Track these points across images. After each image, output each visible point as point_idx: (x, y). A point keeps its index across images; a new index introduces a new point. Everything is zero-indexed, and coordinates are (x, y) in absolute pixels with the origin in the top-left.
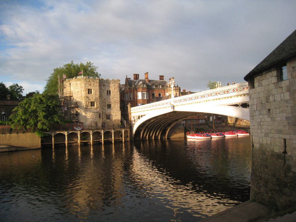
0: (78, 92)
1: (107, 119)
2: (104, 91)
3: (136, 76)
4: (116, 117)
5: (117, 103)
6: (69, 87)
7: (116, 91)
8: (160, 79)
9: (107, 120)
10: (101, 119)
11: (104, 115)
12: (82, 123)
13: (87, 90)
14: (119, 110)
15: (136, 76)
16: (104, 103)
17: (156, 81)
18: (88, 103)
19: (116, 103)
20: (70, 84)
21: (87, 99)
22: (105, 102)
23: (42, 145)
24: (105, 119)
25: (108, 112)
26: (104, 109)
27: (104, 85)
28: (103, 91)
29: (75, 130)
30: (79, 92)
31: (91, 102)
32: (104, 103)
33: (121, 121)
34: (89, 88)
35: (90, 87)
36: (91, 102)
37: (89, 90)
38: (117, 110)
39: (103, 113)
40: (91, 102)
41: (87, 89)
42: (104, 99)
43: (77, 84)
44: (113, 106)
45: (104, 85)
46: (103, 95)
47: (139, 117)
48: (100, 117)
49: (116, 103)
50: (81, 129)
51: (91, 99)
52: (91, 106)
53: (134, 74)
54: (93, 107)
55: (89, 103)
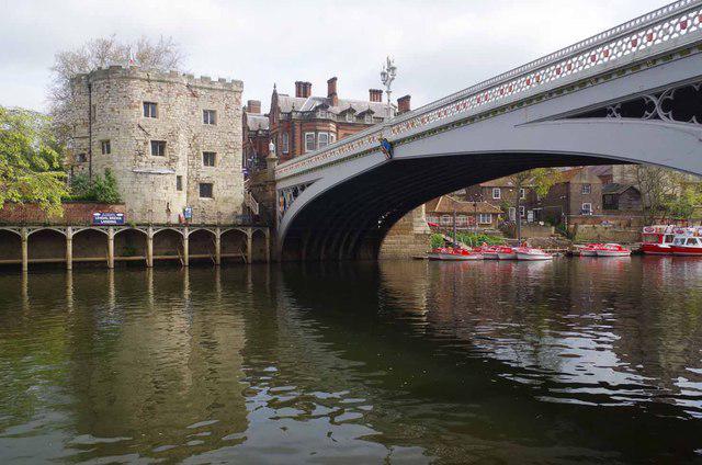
0: (113, 110)
1: (202, 195)
2: (193, 113)
3: (303, 89)
6: (88, 97)
8: (372, 99)
12: (124, 204)
15: (303, 89)
16: (194, 149)
17: (359, 104)
18: (141, 143)
20: (90, 86)
21: (141, 132)
22: (197, 146)
27: (194, 95)
31: (152, 142)
32: (194, 149)
33: (245, 207)
34: (146, 100)
35: (149, 98)
39: (189, 178)
40: (152, 142)
41: (139, 102)
47: (296, 194)
48: (179, 187)
51: (152, 133)
52: (154, 153)
53: (298, 84)
55: (146, 143)
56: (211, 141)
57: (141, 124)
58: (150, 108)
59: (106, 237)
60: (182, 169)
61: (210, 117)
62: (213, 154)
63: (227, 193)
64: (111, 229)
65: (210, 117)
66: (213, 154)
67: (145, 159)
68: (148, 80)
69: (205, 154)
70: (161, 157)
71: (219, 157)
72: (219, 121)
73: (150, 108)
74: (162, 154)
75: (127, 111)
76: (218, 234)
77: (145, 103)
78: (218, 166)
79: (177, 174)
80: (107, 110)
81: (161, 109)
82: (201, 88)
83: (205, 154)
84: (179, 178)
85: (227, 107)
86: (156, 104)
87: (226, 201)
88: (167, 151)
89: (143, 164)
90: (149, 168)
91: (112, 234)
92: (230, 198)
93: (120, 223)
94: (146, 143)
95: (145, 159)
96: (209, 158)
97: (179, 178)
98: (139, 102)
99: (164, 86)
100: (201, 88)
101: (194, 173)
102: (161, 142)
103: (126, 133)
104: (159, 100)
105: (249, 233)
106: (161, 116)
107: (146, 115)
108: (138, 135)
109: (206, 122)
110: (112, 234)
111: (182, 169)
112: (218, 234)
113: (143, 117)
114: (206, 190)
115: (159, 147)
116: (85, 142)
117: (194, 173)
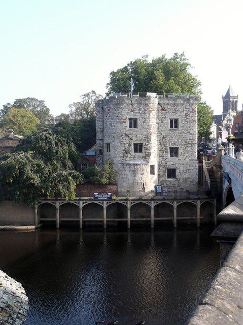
0: (111, 125)
4: (187, 174)
5: (190, 145)
7: (188, 120)
9: (169, 179)
10: (155, 177)
11: (163, 170)
13: (128, 121)
14: (197, 158)
18: (127, 145)
19: (188, 145)
20: (103, 108)
21: (127, 138)
22: (165, 144)
23: (41, 222)
24: (165, 178)
25: (172, 163)
26: (163, 157)
28: (160, 122)
29: (96, 199)
30: (113, 125)
35: (132, 116)
36: (136, 145)
37: (130, 119)
38: (190, 158)
39: (159, 165)
41: (126, 119)
42: (163, 138)
43: (109, 110)
44: (182, 151)
45: (163, 109)
46: (161, 128)
48: (152, 172)
49: (188, 145)
50: (108, 197)
51: (134, 138)
52: (136, 151)
54: (138, 154)
56: (176, 139)
57: (127, 133)
58: (133, 123)
59: (102, 208)
60: (154, 160)
61: (174, 124)
62: (177, 149)
63: (187, 175)
64: (105, 202)
65: (174, 124)
66: (177, 149)
67: (129, 155)
68: (132, 104)
69: (171, 149)
70: (141, 153)
71: (181, 151)
72: (180, 125)
73: (133, 123)
74: (141, 151)
75: (119, 125)
76: (175, 205)
77: (130, 119)
78: (180, 157)
79: (150, 164)
80: (108, 124)
81: (139, 122)
82: (168, 104)
83: (171, 149)
84: (152, 167)
85: (186, 116)
86: (137, 119)
87: (185, 180)
88: (143, 149)
89: (128, 159)
90: (132, 162)
91: (105, 205)
92: (189, 178)
93: (110, 199)
94: (130, 145)
95: (129, 155)
96: (174, 152)
97: (152, 167)
98: (126, 119)
99: (141, 107)
100: (168, 104)
101: (163, 162)
102: (140, 143)
103: (118, 139)
104: (138, 116)
105: (199, 204)
106: (139, 127)
107: (131, 126)
108: (126, 140)
109: (171, 126)
110: (105, 205)
111: (154, 160)
112: (175, 205)
113: (128, 128)
114: (172, 173)
115: (139, 147)
116: (101, 142)
117: (163, 162)
